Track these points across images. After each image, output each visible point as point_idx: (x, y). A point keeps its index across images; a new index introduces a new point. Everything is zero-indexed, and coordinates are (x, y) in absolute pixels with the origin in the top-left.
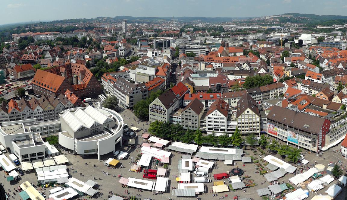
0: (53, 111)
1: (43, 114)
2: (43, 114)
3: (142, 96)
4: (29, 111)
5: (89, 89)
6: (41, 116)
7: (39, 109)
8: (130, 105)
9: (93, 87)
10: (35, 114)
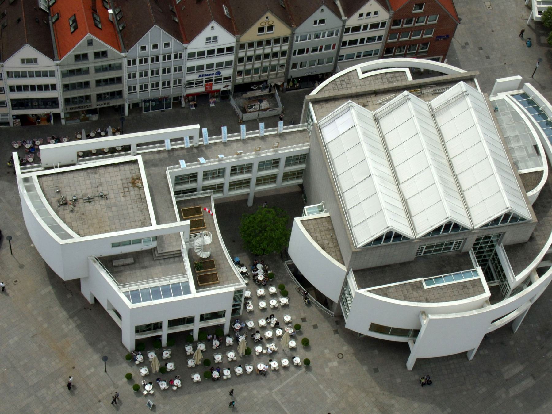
1: (231, 57)
2: (231, 57)
6: (220, 65)
7: (215, 38)
10: (191, 56)
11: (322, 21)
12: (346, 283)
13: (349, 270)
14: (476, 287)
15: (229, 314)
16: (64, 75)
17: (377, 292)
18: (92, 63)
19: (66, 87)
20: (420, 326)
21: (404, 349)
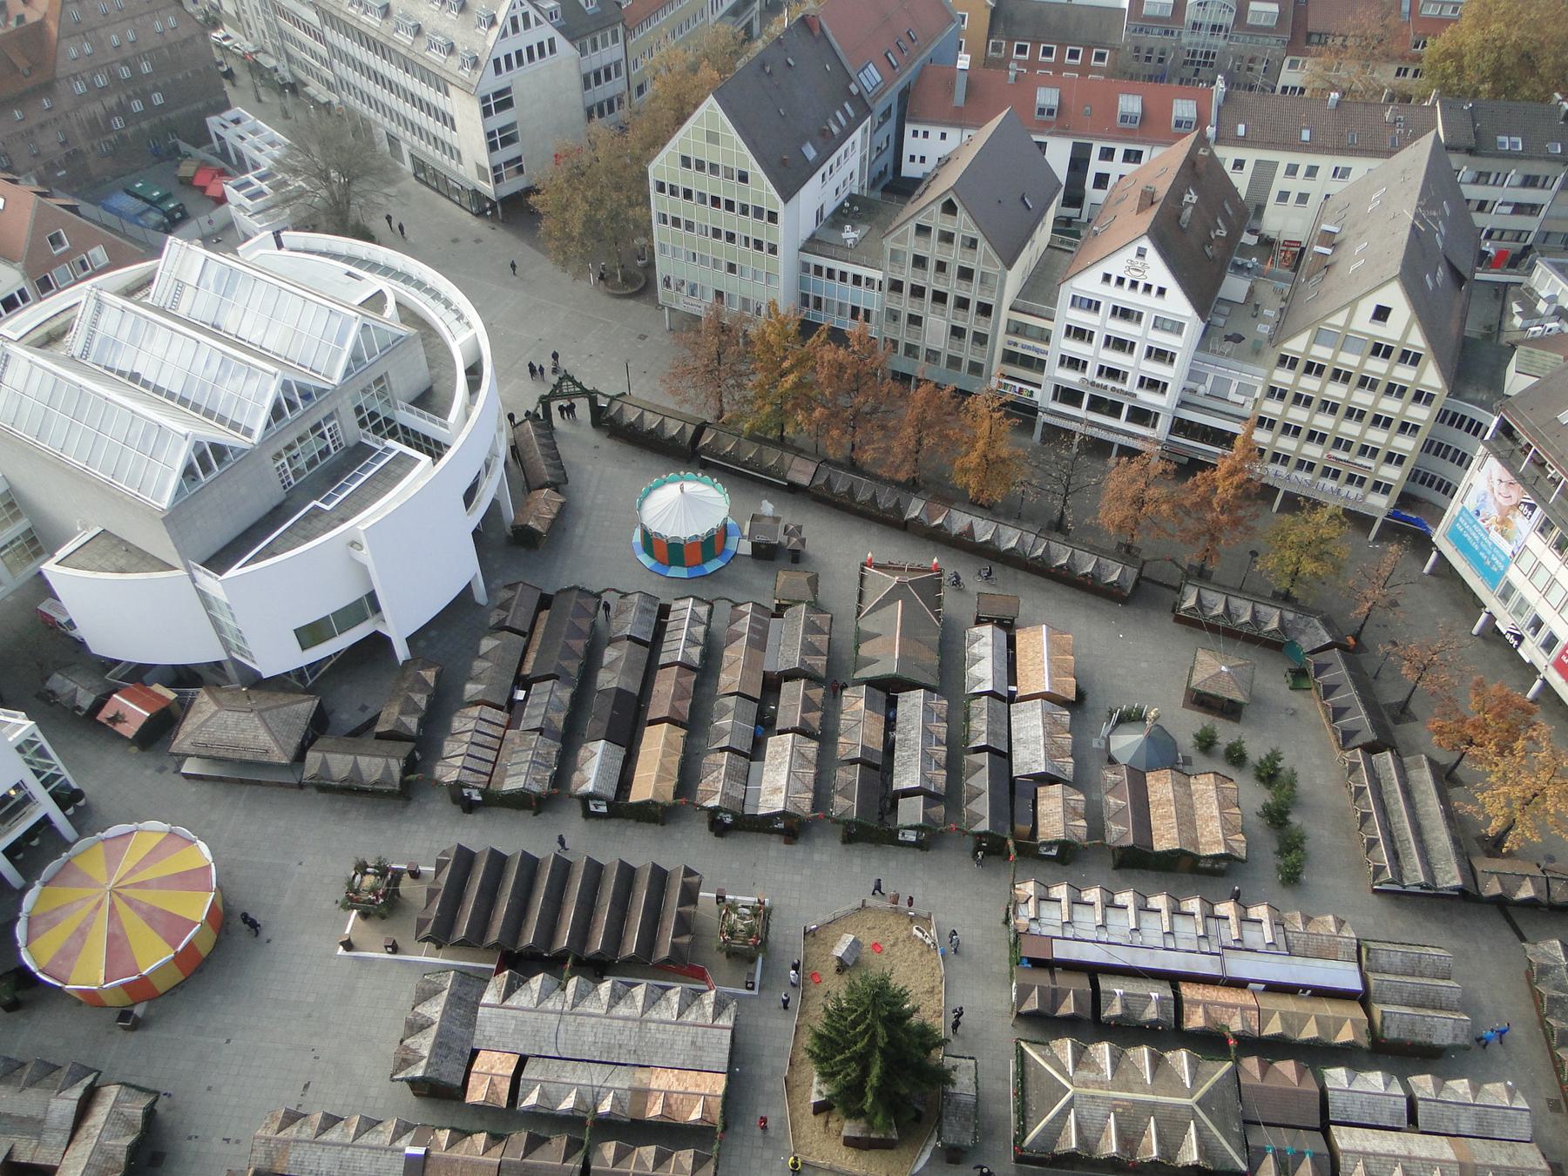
3: (577, 82)
5: (101, 81)
8: (498, 179)
9: (128, 52)
12: (202, 595)
13: (188, 568)
14: (404, 463)
15: (35, 786)
17: (254, 560)
20: (363, 569)
21: (378, 644)
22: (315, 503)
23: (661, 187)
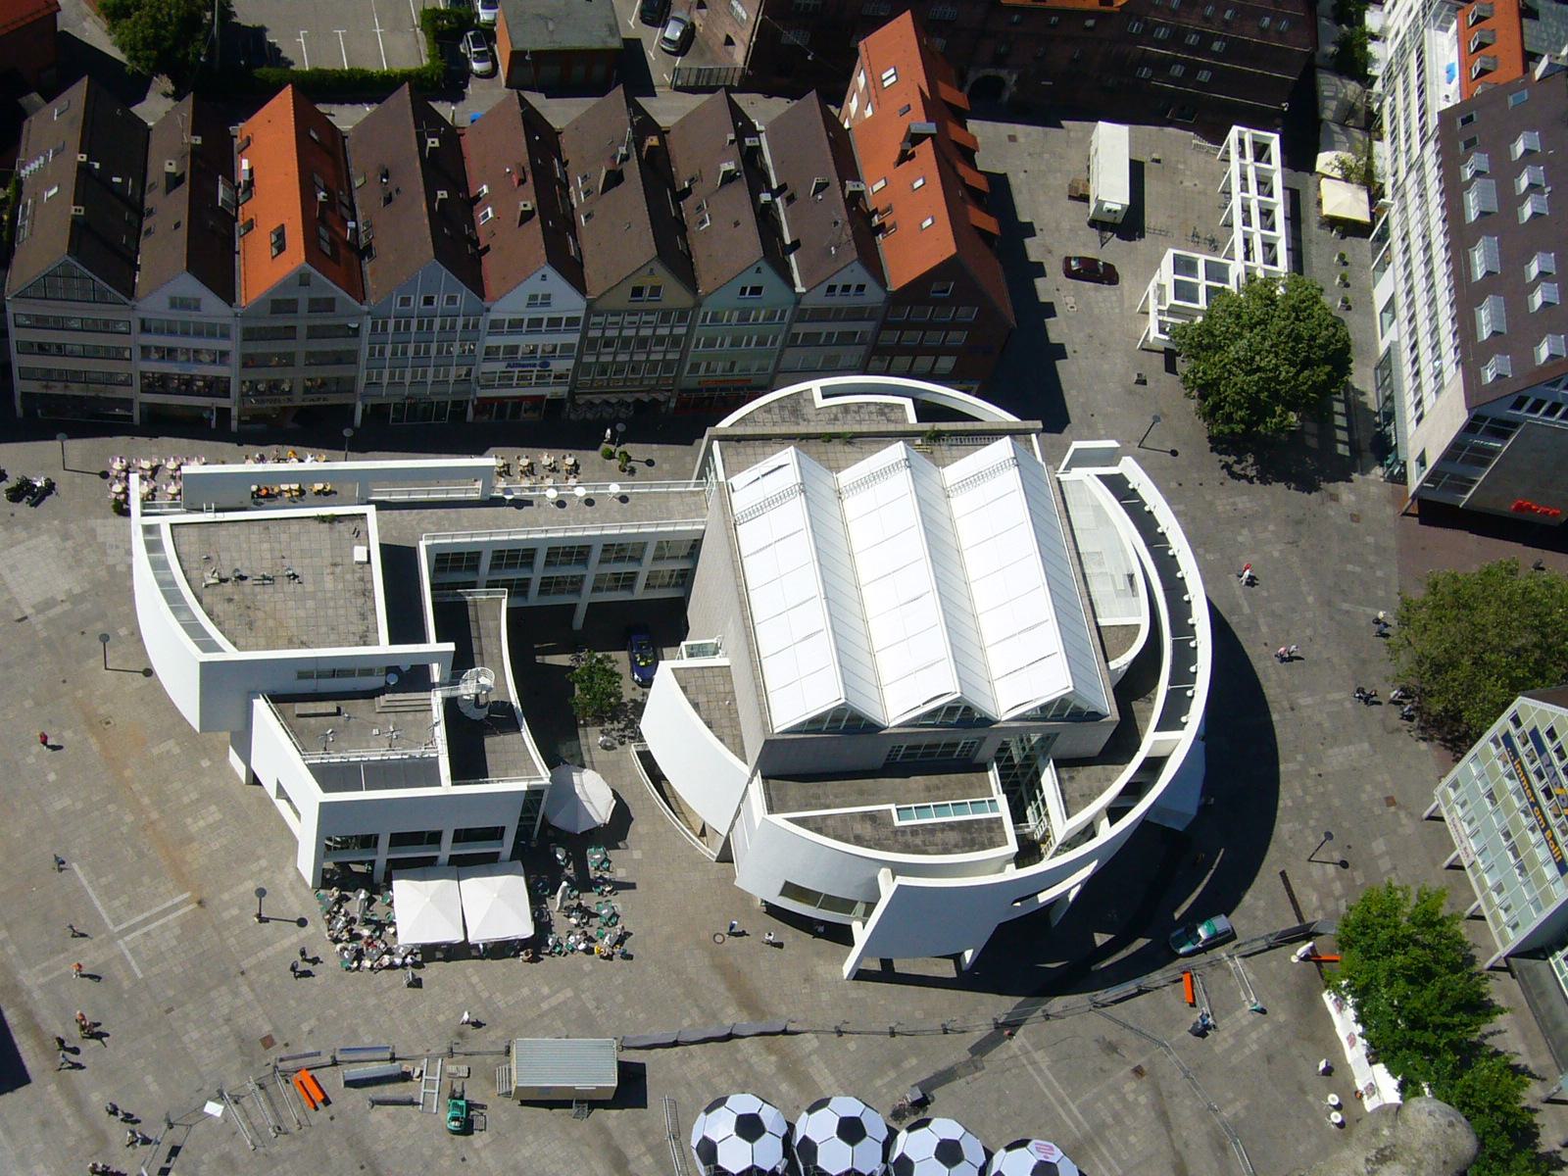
0: (682, 317)
1: (574, 338)
4: (452, 300)
7: (547, 297)
10: (496, 326)
11: (756, 290)
13: (754, 774)
16: (250, 335)
18: (302, 321)
19: (248, 362)
22: (892, 807)
23: (1516, 721)
